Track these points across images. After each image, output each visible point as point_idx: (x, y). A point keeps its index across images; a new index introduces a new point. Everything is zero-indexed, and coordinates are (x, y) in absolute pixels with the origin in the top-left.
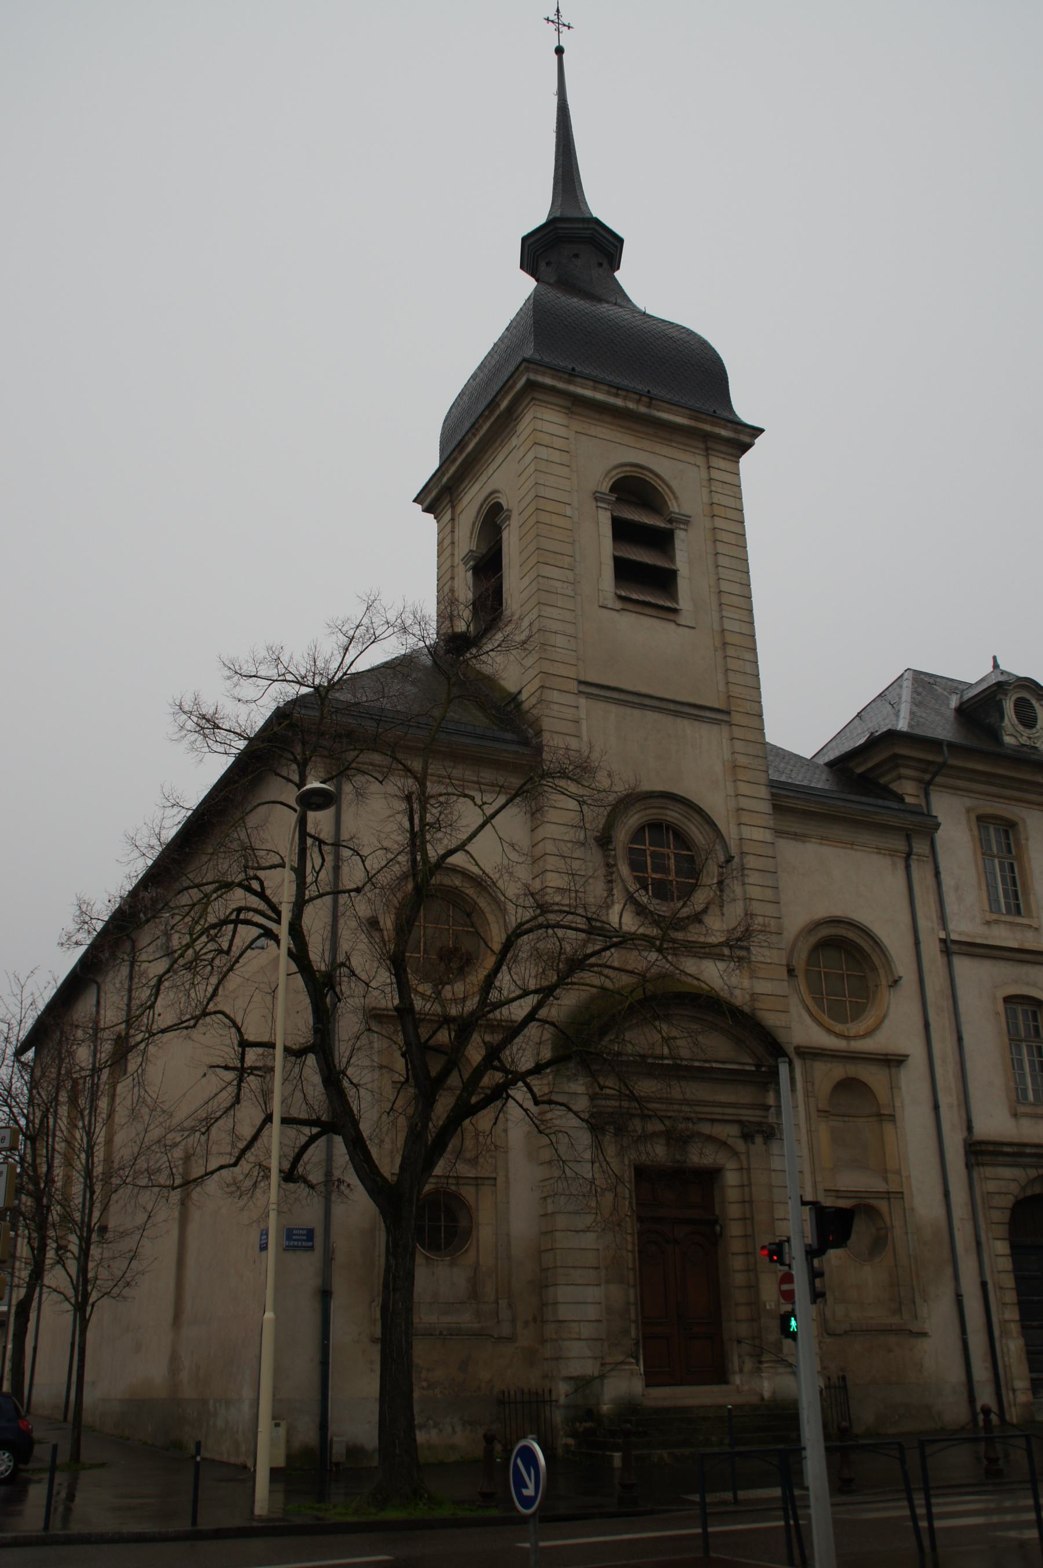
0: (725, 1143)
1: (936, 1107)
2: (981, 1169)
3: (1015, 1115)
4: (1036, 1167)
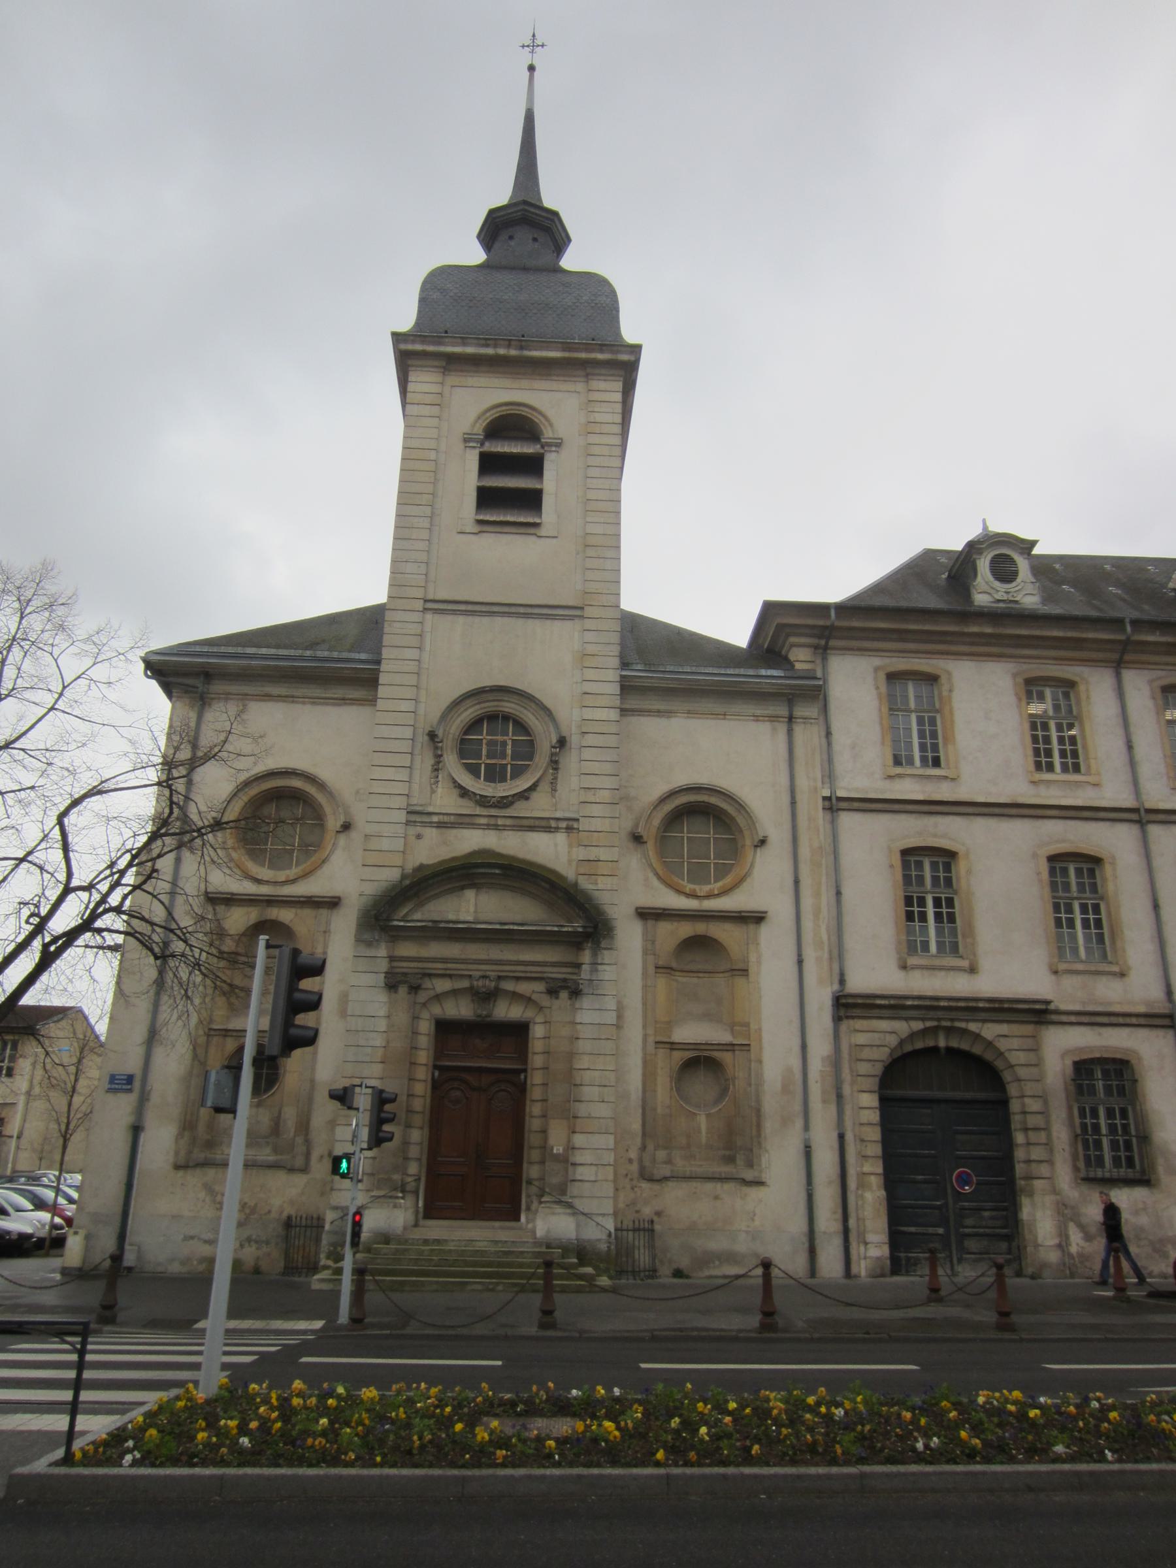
0: (529, 999)
1: (800, 962)
2: (851, 1022)
3: (904, 967)
4: (923, 1020)
